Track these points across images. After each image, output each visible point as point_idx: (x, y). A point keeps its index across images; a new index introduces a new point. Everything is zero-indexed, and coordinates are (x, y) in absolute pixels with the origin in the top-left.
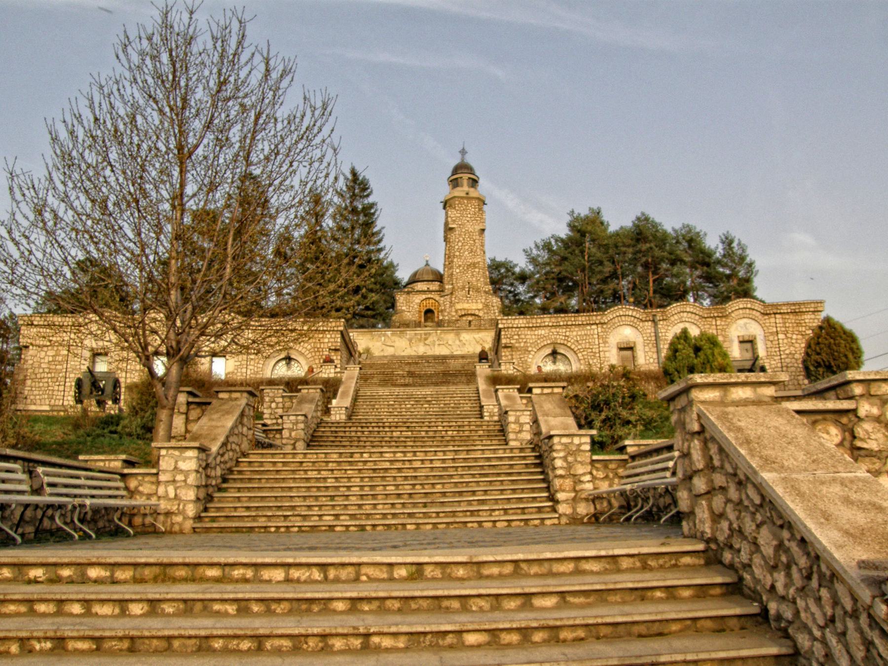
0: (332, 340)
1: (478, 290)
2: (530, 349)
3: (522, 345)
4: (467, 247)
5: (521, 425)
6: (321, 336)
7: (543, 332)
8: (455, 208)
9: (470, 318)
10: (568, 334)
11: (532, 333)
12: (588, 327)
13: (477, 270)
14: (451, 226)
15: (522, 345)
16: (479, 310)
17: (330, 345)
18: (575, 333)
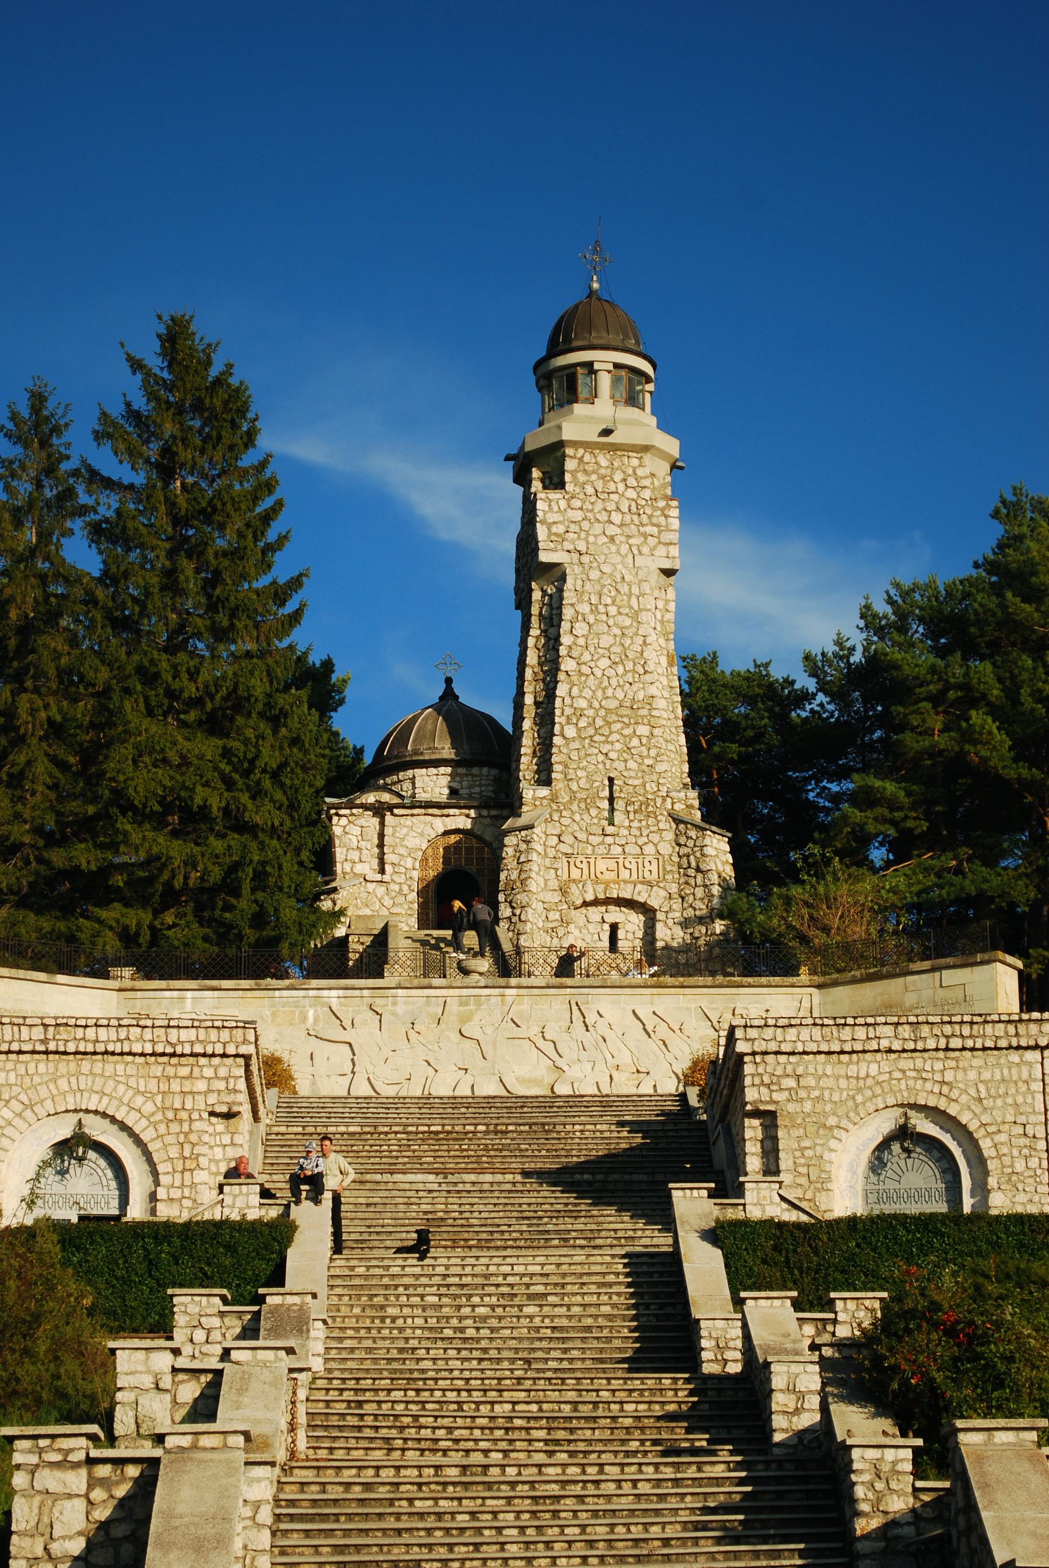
0: (221, 1085)
1: (645, 808)
2: (832, 1121)
3: (808, 1106)
4: (606, 641)
5: (801, 1396)
6: (184, 1071)
7: (874, 1069)
8: (561, 485)
9: (615, 914)
10: (949, 1076)
11: (841, 1070)
12: (1014, 1057)
13: (643, 730)
14: (544, 557)
15: (808, 1106)
16: (650, 884)
17: (212, 1099)
18: (972, 1075)
